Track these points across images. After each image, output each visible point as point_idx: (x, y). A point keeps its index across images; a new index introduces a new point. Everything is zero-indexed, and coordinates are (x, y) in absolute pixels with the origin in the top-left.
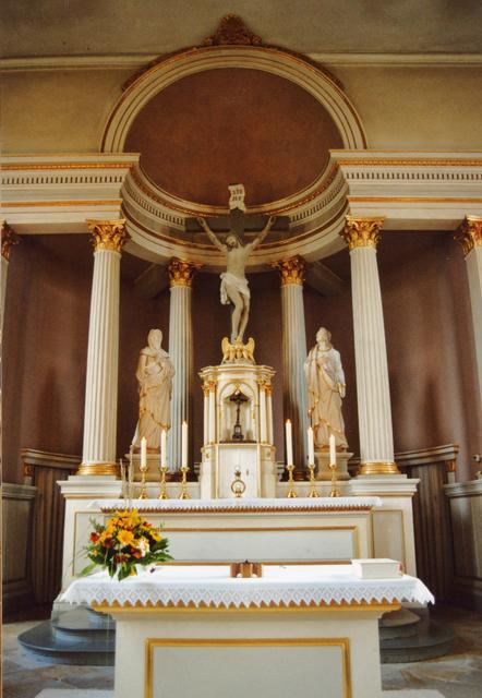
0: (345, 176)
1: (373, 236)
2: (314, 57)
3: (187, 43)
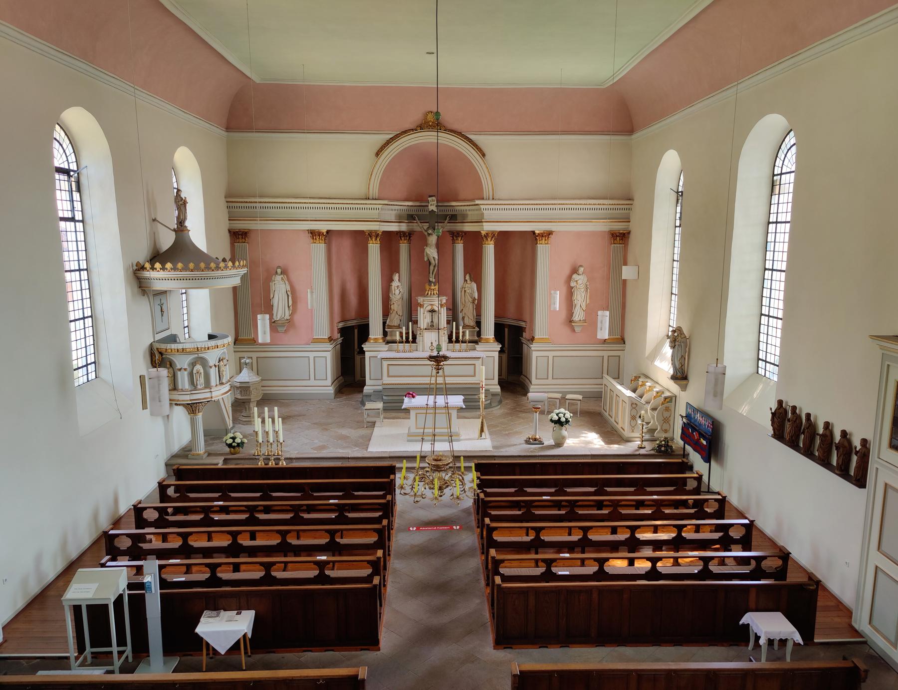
0: (482, 210)
1: (493, 239)
2: (471, 137)
3: (407, 126)
